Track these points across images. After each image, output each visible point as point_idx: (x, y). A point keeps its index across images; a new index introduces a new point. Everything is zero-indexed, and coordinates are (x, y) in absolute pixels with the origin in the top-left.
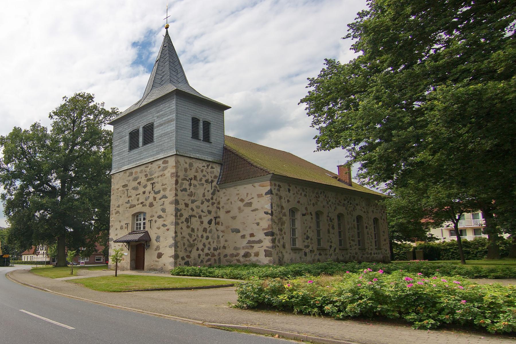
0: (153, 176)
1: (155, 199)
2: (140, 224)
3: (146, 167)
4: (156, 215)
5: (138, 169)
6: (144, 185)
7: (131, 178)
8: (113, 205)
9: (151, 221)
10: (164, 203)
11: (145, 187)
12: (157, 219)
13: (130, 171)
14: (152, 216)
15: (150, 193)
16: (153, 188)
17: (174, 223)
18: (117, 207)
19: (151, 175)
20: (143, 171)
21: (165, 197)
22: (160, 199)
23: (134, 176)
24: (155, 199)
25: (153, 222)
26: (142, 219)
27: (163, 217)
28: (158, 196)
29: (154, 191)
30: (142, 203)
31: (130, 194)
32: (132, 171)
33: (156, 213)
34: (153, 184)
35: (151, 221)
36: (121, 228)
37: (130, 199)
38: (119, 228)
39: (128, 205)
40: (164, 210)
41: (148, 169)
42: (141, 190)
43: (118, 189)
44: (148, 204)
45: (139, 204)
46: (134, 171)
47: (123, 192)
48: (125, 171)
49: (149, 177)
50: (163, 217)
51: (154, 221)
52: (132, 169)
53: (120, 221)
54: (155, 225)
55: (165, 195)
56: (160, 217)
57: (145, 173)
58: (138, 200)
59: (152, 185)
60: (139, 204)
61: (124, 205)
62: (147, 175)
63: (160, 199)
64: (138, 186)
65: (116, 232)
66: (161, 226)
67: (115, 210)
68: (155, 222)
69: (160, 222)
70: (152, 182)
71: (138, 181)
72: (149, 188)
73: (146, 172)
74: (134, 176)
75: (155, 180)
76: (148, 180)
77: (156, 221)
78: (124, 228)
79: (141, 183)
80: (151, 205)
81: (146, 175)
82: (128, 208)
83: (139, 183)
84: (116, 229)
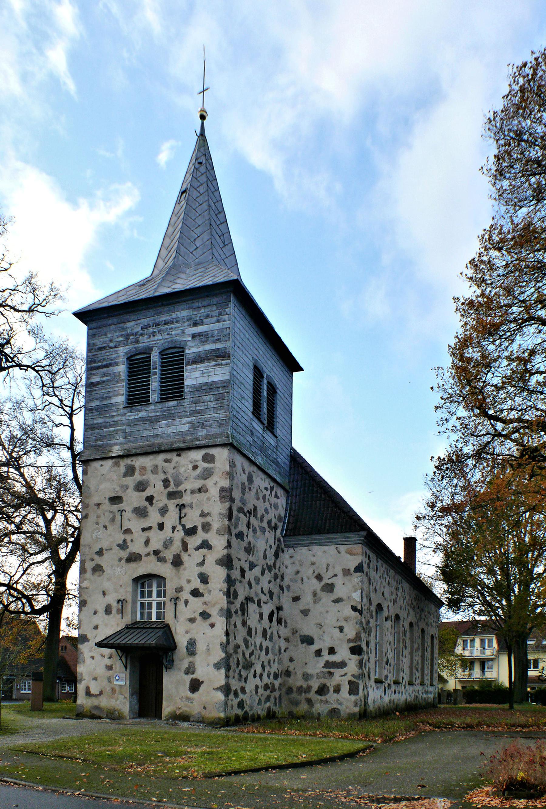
0: (181, 488)
2: (150, 605)
4: (188, 588)
5: (147, 462)
6: (161, 505)
8: (85, 546)
10: (204, 560)
11: (163, 511)
12: (191, 598)
13: (128, 461)
14: (179, 590)
15: (174, 528)
16: (180, 518)
17: (225, 612)
18: (97, 553)
19: (178, 484)
20: (160, 468)
21: (205, 545)
22: (197, 549)
23: (137, 477)
25: (181, 605)
26: (154, 594)
27: (202, 595)
28: (194, 541)
29: (184, 526)
32: (133, 463)
33: (189, 581)
34: (182, 507)
37: (128, 537)
39: (125, 554)
40: (204, 579)
42: (154, 518)
45: (148, 554)
46: (138, 462)
47: (111, 516)
48: (117, 460)
50: (202, 595)
51: (183, 600)
52: (134, 459)
54: (185, 612)
55: (207, 541)
56: (195, 593)
58: (147, 542)
59: (180, 510)
61: (113, 551)
62: (169, 481)
63: (197, 549)
64: (146, 507)
67: (93, 560)
69: (196, 604)
70: (180, 501)
71: (148, 492)
74: (137, 477)
75: (187, 499)
76: (171, 495)
77: (186, 602)
79: (154, 501)
81: (166, 483)
82: (123, 561)
83: (150, 499)
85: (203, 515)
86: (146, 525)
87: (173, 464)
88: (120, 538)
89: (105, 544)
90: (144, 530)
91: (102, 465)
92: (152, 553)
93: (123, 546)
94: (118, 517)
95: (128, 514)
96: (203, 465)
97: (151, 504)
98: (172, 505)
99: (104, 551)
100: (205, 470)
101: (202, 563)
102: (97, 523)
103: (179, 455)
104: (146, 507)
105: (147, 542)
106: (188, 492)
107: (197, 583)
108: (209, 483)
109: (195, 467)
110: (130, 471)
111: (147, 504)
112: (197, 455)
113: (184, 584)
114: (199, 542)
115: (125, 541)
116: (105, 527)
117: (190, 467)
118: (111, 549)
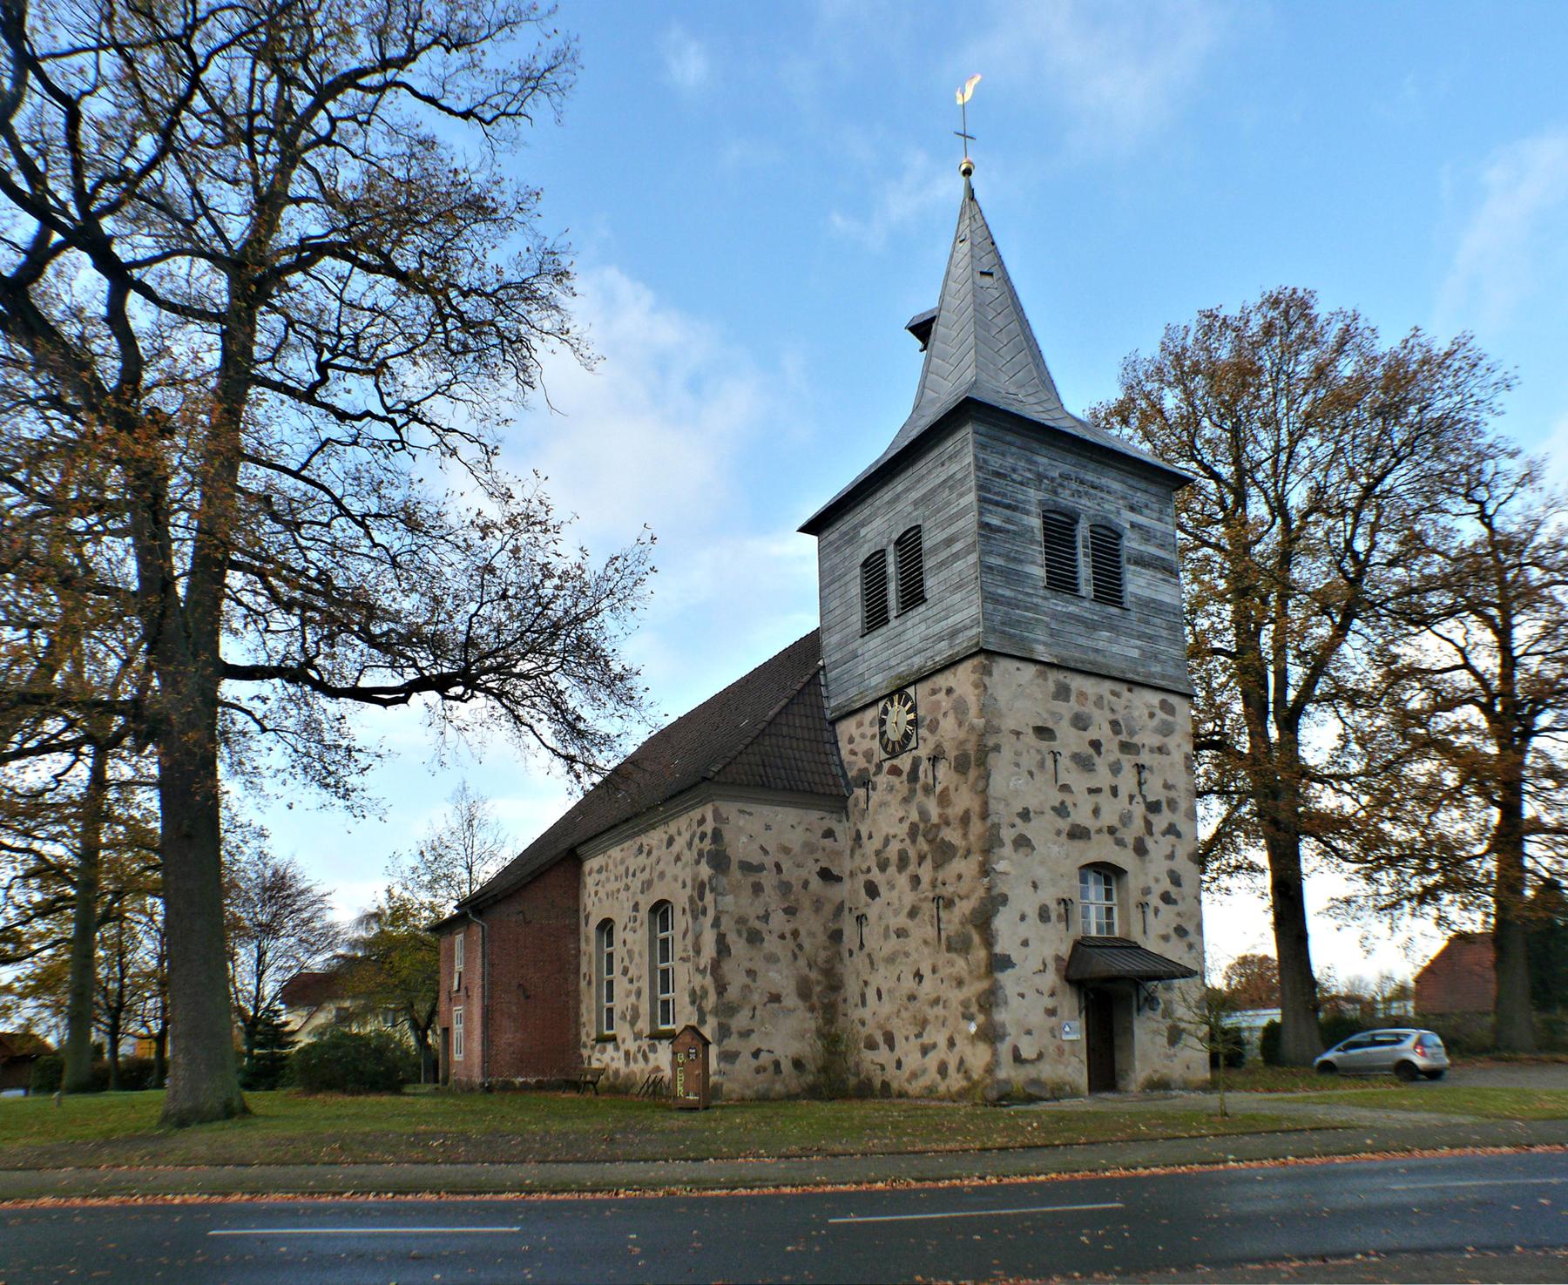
0: (1136, 740)
1: (1148, 825)
3: (1114, 693)
4: (1158, 890)
6: (1112, 758)
7: (1060, 706)
9: (1143, 906)
10: (1173, 852)
11: (1115, 769)
12: (1161, 905)
13: (1060, 676)
14: (1147, 891)
15: (1131, 797)
18: (1020, 815)
19: (1132, 733)
20: (1106, 702)
24: (1148, 825)
27: (1174, 902)
28: (1160, 822)
29: (1144, 797)
30: (1112, 831)
31: (1064, 778)
32: (1068, 681)
34: (1140, 768)
35: (1143, 906)
36: (1044, 915)
38: (1033, 914)
39: (1064, 825)
41: (1119, 704)
42: (1103, 778)
43: (1018, 734)
44: (1130, 841)
46: (1077, 683)
47: (1039, 757)
49: (1124, 737)
50: (1174, 902)
52: (1069, 675)
53: (1035, 886)
57: (1111, 717)
60: (1099, 831)
64: (1091, 756)
65: (1024, 930)
66: (1171, 931)
67: (1013, 826)
68: (1156, 914)
71: (1092, 734)
72: (1127, 782)
73: (1113, 710)
75: (1145, 758)
76: (1126, 747)
77: (1156, 911)
78: (1054, 916)
80: (1141, 849)
82: (1064, 835)
83: (1096, 745)
84: (1023, 918)
85: (1167, 786)
86: (1094, 785)
87: (1123, 701)
88: (1056, 798)
89: (1032, 804)
90: (1091, 791)
91: (1018, 669)
92: (1105, 829)
93: (1061, 811)
94: (1049, 763)
95: (1064, 761)
96: (1161, 715)
97: (1099, 753)
98: (1127, 761)
99: (1032, 814)
100: (1164, 722)
101: (1171, 856)
102: (1017, 765)
103: (1130, 690)
104: (1091, 756)
105: (1096, 812)
106: (1147, 749)
107: (1166, 885)
108: (1171, 742)
109: (1152, 715)
110: (1063, 693)
111: (1091, 751)
112: (1154, 698)
113: (1152, 884)
114: (1164, 826)
115: (1063, 803)
116: (1031, 774)
117: (1146, 712)
118: (1042, 813)
